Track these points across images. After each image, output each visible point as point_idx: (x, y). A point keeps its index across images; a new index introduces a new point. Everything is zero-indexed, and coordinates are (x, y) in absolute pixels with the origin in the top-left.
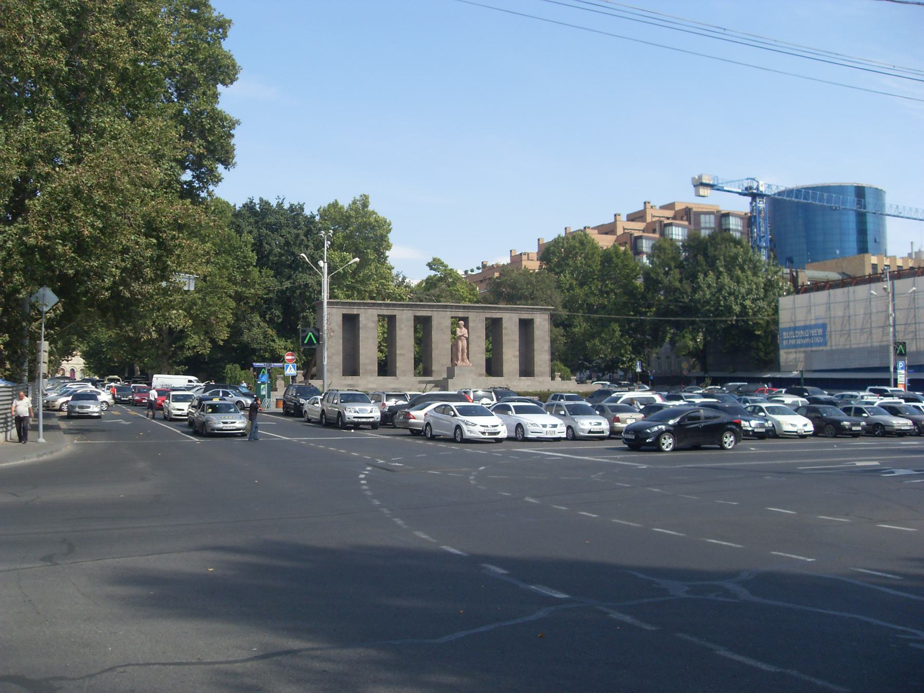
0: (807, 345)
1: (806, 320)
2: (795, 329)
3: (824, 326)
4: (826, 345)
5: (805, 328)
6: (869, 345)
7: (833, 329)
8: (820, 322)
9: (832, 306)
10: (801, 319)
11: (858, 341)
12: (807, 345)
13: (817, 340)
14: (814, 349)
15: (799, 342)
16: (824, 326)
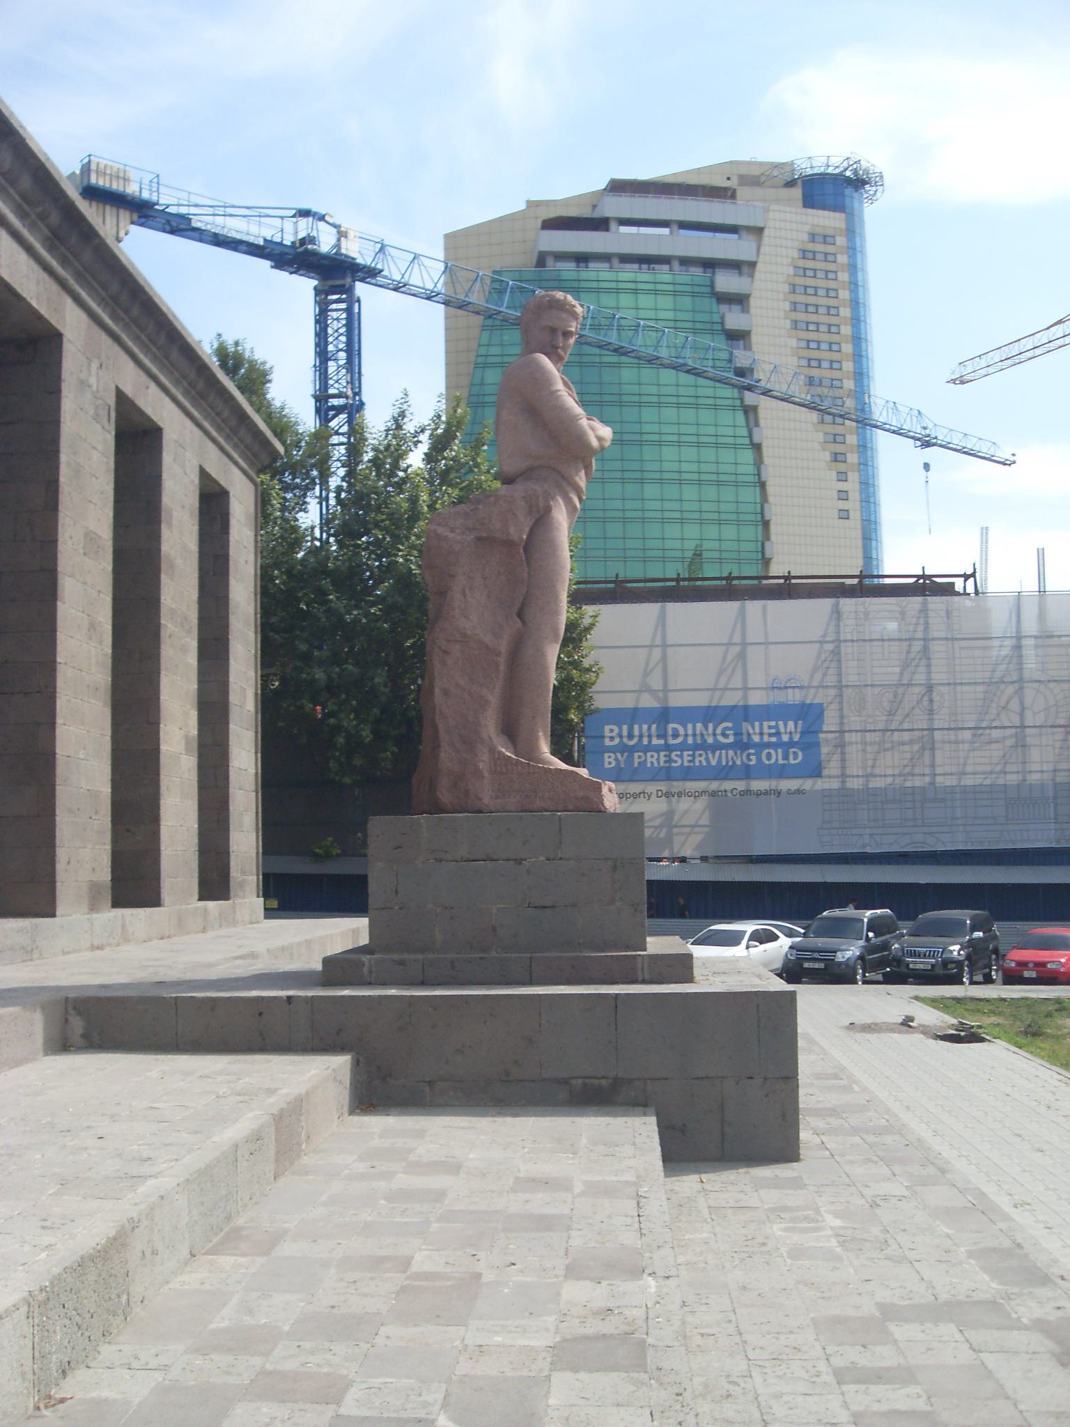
0: (724, 773)
1: (645, 688)
2: (664, 715)
3: (809, 715)
4: (816, 772)
5: (710, 714)
6: (1012, 779)
7: (854, 721)
8: (794, 697)
9: (846, 649)
10: (692, 682)
11: (967, 763)
12: (724, 773)
13: (777, 757)
14: (759, 785)
15: (681, 760)
16: (809, 715)
